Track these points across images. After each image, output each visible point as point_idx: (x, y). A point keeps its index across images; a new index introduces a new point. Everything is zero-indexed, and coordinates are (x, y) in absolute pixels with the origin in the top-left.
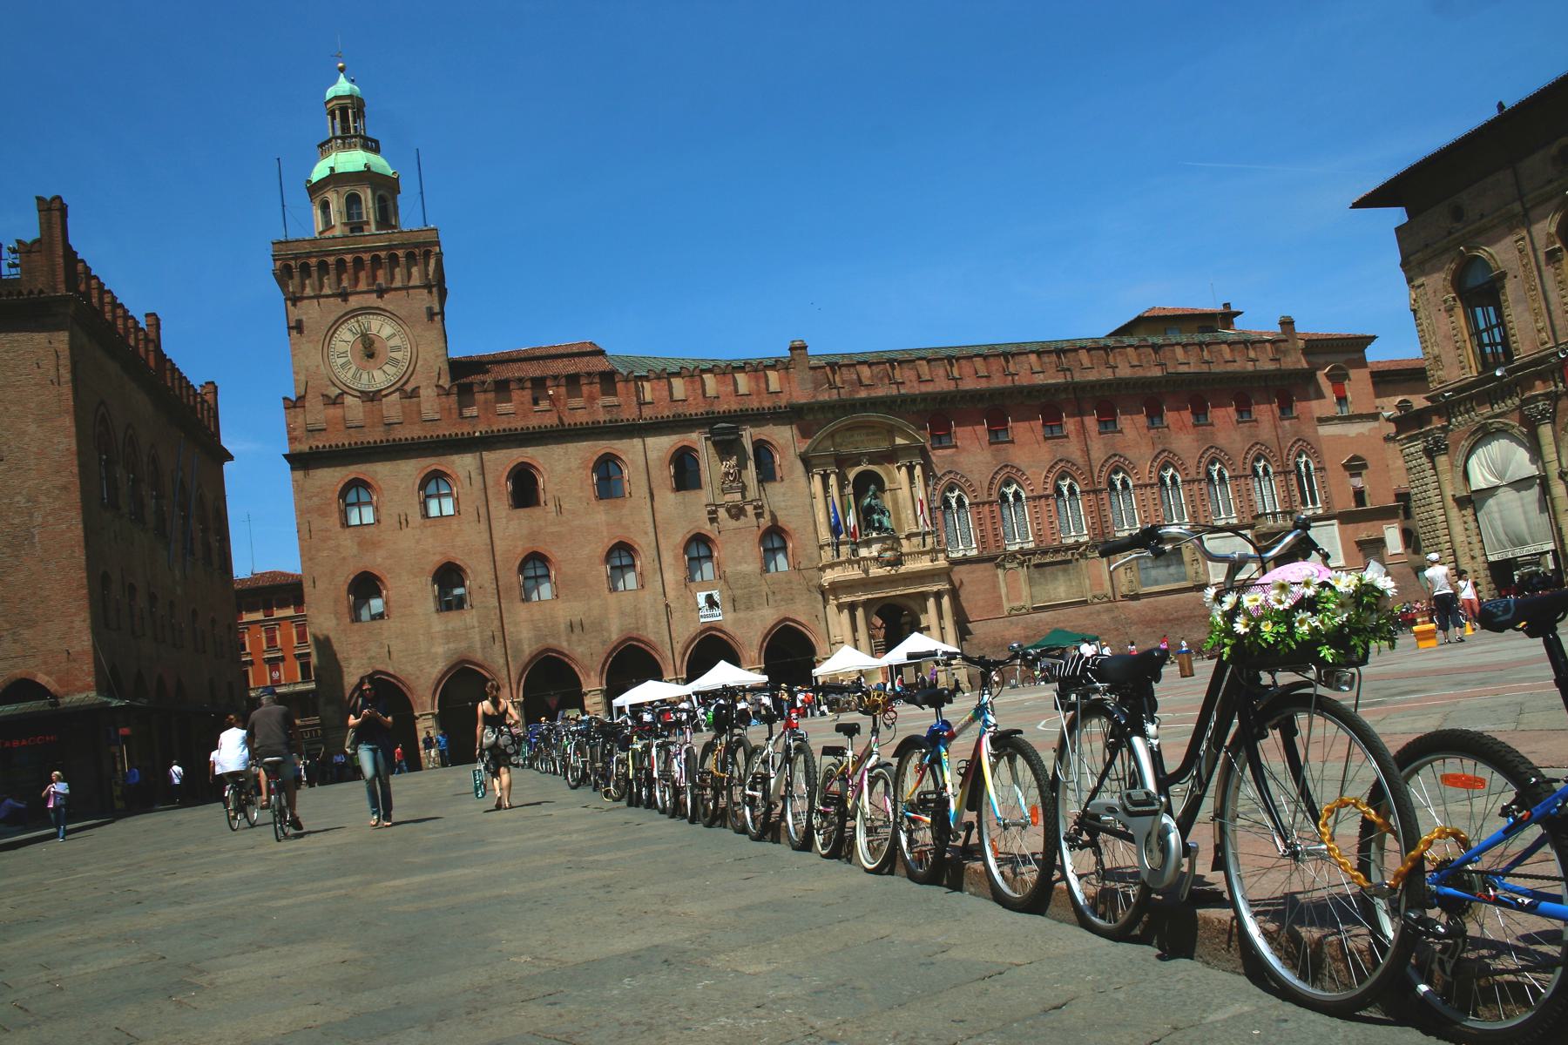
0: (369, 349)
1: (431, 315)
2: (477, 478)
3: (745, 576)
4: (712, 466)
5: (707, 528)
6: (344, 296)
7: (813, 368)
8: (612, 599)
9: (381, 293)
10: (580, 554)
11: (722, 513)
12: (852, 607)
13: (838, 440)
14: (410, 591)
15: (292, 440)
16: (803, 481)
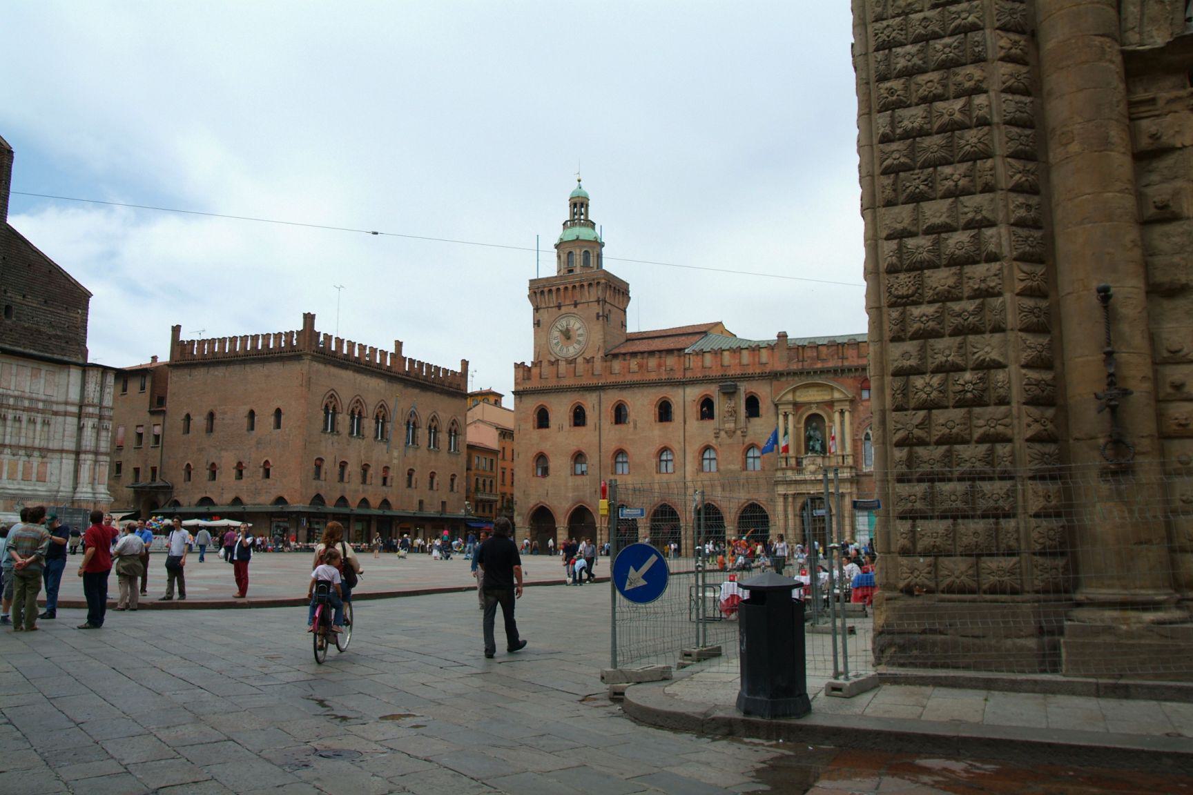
0: (567, 335)
1: (598, 316)
2: (597, 407)
3: (732, 471)
4: (721, 405)
5: (713, 442)
6: (559, 307)
7: (790, 349)
8: (657, 477)
9: (576, 305)
10: (642, 452)
11: (722, 433)
12: (785, 496)
13: (798, 393)
14: (560, 464)
15: (516, 384)
16: (774, 419)
